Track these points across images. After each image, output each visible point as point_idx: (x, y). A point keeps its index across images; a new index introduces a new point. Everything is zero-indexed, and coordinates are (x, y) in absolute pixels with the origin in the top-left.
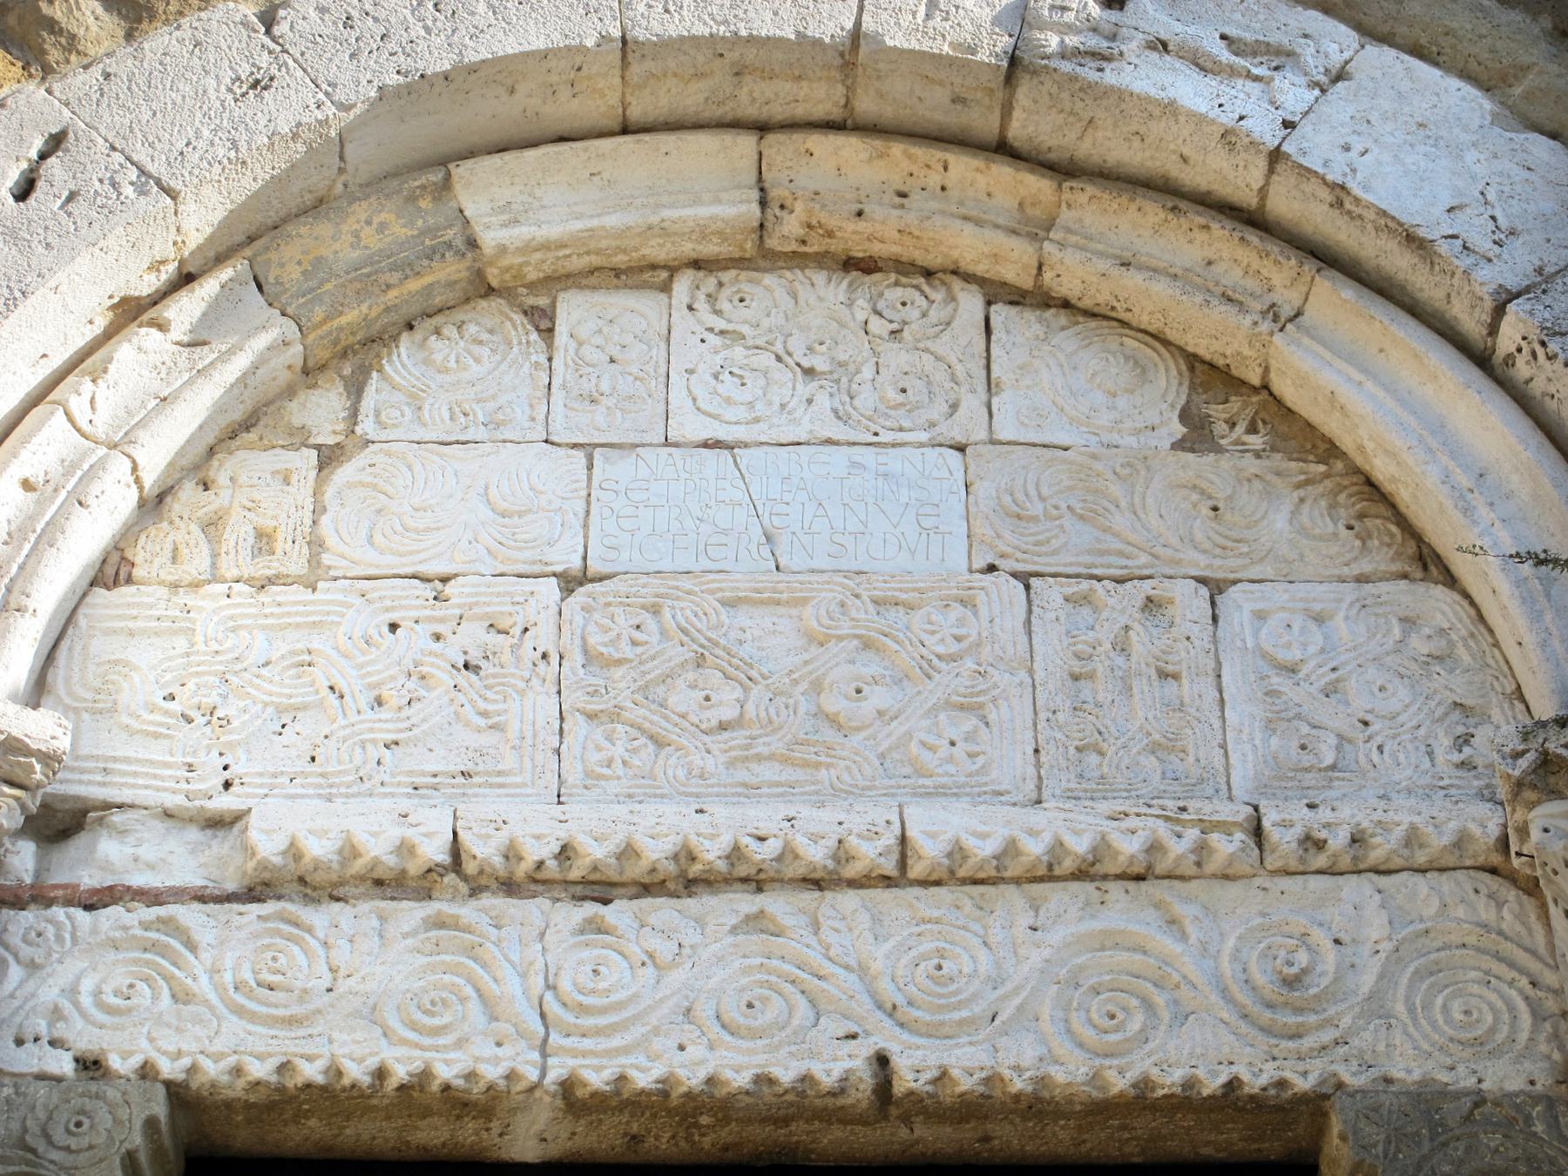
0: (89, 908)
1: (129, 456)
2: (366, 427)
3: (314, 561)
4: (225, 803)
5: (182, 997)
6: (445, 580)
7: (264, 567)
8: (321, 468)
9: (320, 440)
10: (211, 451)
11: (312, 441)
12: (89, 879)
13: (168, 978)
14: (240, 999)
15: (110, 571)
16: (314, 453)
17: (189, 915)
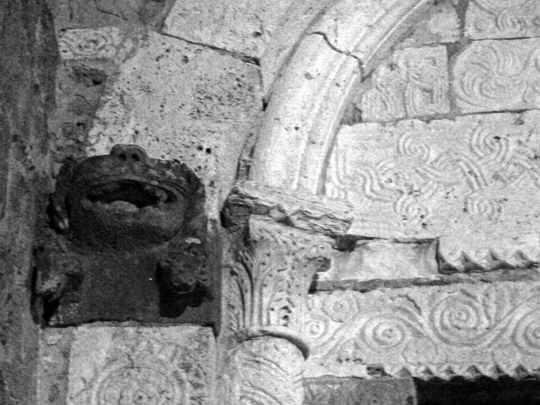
0: (363, 291)
1: (355, 57)
2: (470, 31)
3: (453, 105)
4: (424, 235)
5: (418, 334)
6: (520, 111)
7: (430, 109)
8: (449, 57)
9: (447, 40)
10: (392, 49)
11: (443, 41)
12: (362, 277)
13: (409, 326)
14: (445, 335)
15: (350, 115)
16: (444, 48)
17: (414, 292)
